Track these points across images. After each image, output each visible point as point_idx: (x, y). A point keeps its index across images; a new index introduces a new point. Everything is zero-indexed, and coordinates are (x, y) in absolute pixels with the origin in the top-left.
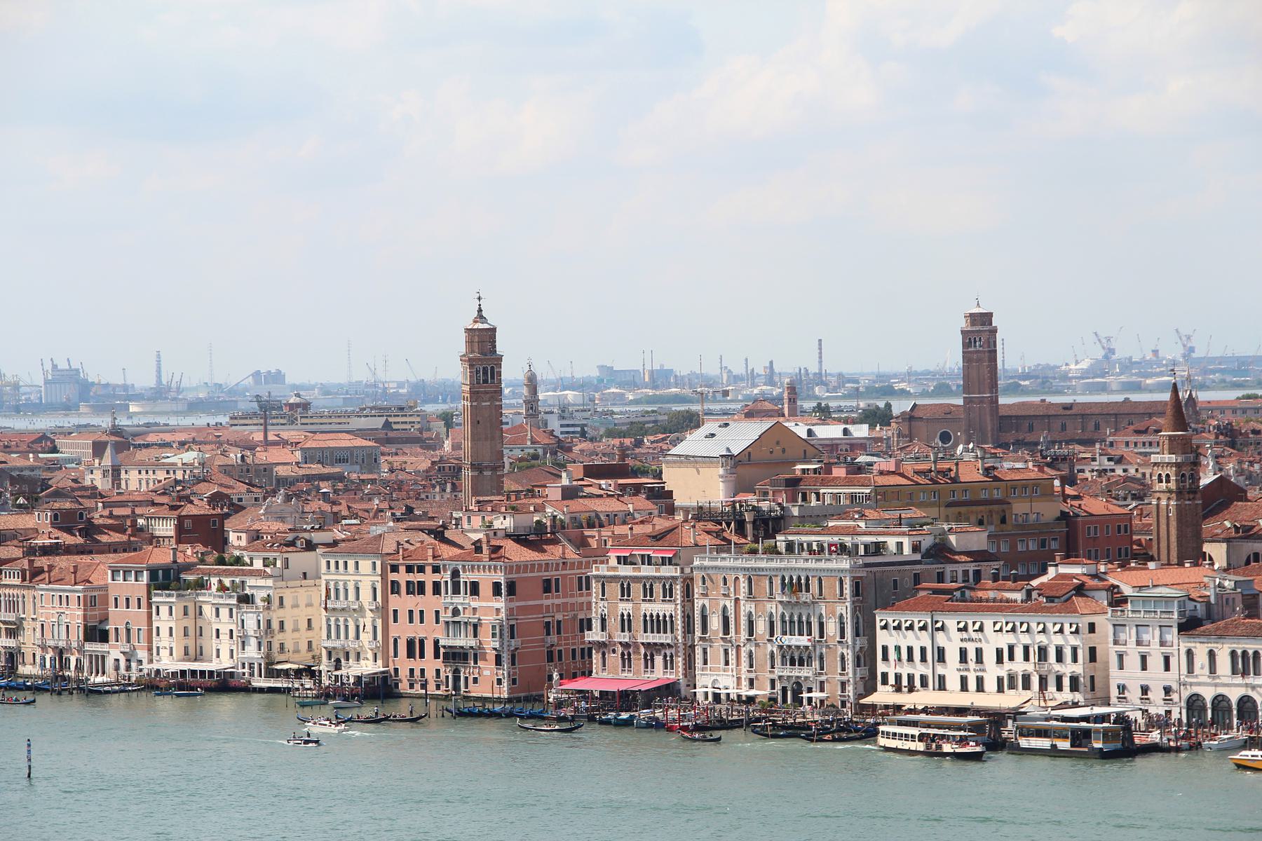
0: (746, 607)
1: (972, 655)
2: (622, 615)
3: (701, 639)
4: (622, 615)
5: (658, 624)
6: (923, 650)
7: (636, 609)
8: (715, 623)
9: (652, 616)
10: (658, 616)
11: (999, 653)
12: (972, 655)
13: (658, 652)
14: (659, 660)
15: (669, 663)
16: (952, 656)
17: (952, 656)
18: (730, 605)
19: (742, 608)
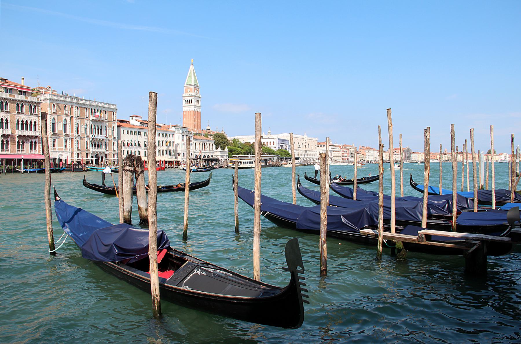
8: (59, 127)
14: (27, 145)
17: (142, 145)
18: (68, 119)
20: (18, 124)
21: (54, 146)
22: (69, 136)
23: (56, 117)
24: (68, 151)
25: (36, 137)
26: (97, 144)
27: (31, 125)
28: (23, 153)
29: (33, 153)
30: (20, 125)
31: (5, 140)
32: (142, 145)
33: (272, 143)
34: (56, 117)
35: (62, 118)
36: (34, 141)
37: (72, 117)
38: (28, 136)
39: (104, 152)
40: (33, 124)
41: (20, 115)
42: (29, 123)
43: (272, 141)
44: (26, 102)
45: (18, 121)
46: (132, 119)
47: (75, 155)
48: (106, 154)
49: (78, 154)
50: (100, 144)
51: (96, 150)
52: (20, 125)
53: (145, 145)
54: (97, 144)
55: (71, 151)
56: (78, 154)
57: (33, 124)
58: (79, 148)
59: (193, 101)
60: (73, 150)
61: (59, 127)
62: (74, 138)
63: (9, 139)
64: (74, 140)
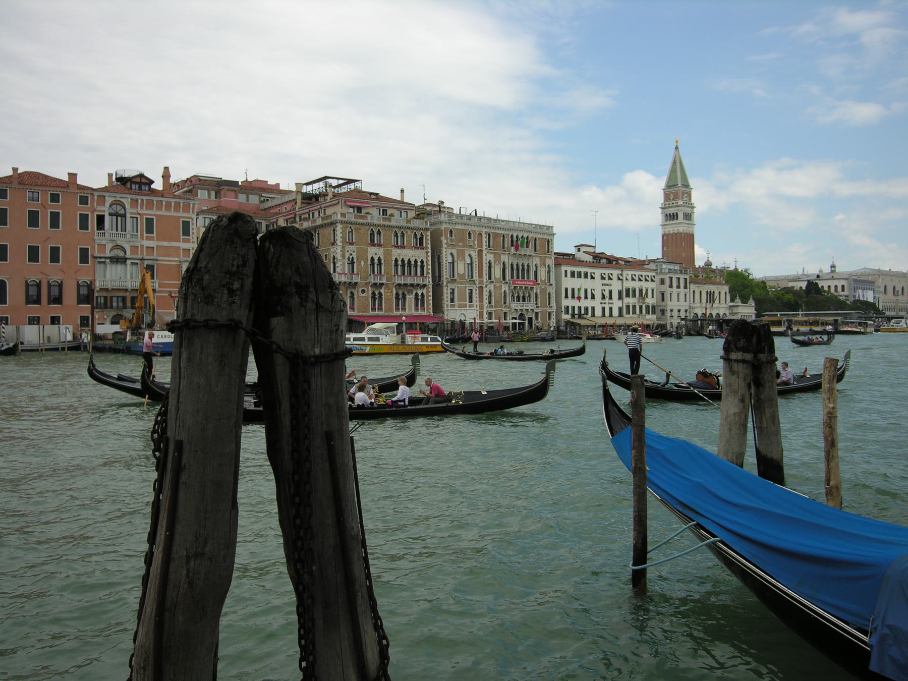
0: (488, 257)
1: (607, 294)
2: (372, 259)
4: (372, 259)
5: (407, 267)
7: (388, 254)
8: (461, 268)
9: (403, 261)
10: (409, 261)
13: (410, 292)
14: (410, 298)
15: (419, 301)
17: (598, 296)
18: (474, 255)
19: (484, 257)
20: (396, 265)
21: (452, 300)
23: (454, 252)
25: (424, 286)
26: (521, 295)
27: (416, 266)
28: (404, 313)
29: (420, 312)
30: (399, 267)
31: (377, 293)
32: (598, 296)
33: (840, 289)
36: (420, 293)
37: (480, 252)
38: (412, 285)
39: (533, 310)
40: (419, 264)
41: (399, 251)
42: (413, 263)
43: (839, 284)
44: (408, 228)
45: (396, 260)
46: (579, 250)
47: (485, 316)
48: (537, 314)
49: (490, 313)
50: (527, 295)
52: (399, 267)
53: (603, 297)
54: (521, 295)
56: (490, 313)
57: (419, 264)
58: (493, 304)
59: (681, 216)
60: (482, 307)
63: (382, 291)
64: (485, 289)
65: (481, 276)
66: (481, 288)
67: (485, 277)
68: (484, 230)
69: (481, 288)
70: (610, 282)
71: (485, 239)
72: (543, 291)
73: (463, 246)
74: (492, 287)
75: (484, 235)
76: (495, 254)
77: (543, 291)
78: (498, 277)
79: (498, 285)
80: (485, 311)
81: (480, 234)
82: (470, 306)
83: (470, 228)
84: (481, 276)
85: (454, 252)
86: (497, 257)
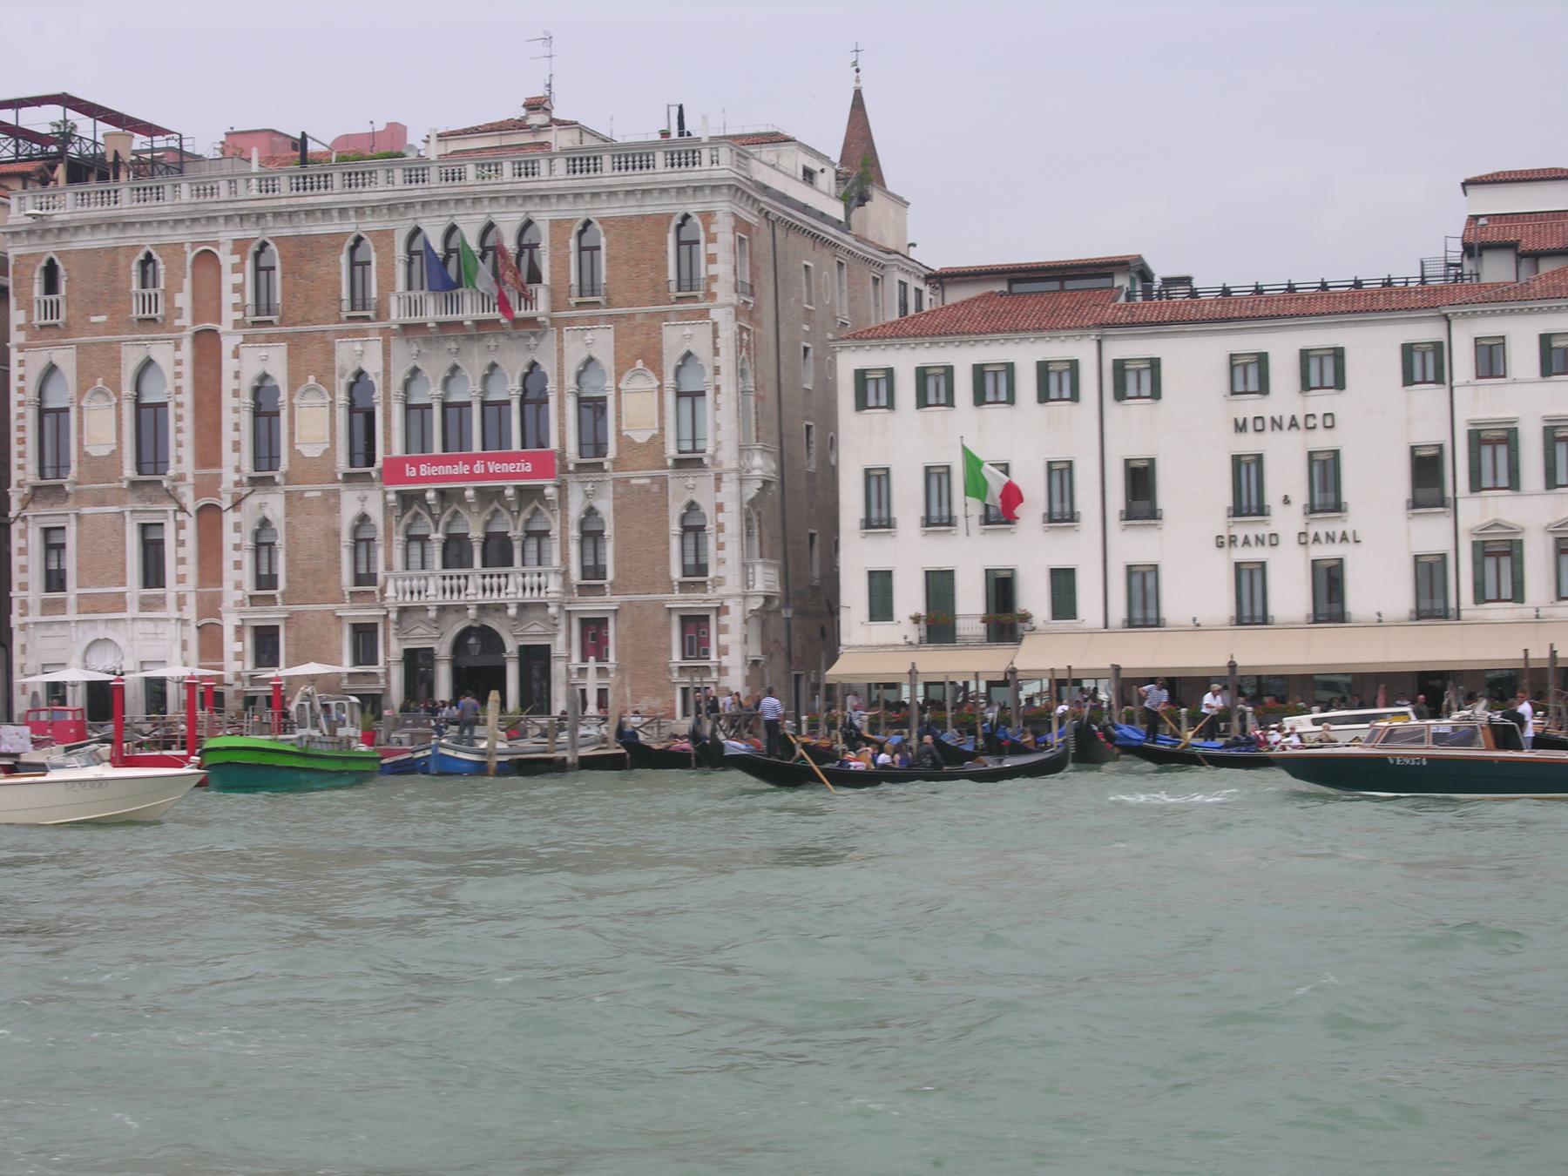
1: (1286, 478)
3: (37, 494)
6: (1060, 474)
8: (101, 429)
11: (1427, 472)
12: (1286, 478)
16: (1194, 494)
17: (1194, 494)
19: (228, 365)
21: (55, 580)
22: (171, 495)
24: (171, 611)
34: (66, 358)
35: (116, 362)
37: (207, 344)
51: (475, 586)
55: (190, 612)
60: (210, 606)
61: (101, 429)
62: (226, 504)
64: (229, 518)
65: (208, 453)
66: (209, 517)
67: (236, 461)
68: (227, 235)
69: (209, 517)
70: (1321, 402)
71: (234, 280)
72: (642, 505)
73: (108, 329)
74: (274, 505)
75: (227, 259)
76: (296, 345)
77: (642, 505)
78: (312, 451)
79: (313, 492)
80: (230, 622)
81: (207, 258)
82: (145, 605)
83: (146, 240)
84: (208, 453)
85: (66, 358)
86: (310, 358)
